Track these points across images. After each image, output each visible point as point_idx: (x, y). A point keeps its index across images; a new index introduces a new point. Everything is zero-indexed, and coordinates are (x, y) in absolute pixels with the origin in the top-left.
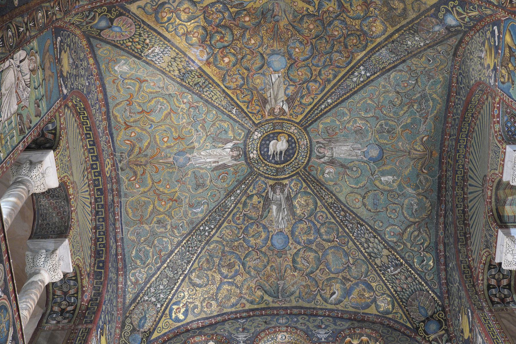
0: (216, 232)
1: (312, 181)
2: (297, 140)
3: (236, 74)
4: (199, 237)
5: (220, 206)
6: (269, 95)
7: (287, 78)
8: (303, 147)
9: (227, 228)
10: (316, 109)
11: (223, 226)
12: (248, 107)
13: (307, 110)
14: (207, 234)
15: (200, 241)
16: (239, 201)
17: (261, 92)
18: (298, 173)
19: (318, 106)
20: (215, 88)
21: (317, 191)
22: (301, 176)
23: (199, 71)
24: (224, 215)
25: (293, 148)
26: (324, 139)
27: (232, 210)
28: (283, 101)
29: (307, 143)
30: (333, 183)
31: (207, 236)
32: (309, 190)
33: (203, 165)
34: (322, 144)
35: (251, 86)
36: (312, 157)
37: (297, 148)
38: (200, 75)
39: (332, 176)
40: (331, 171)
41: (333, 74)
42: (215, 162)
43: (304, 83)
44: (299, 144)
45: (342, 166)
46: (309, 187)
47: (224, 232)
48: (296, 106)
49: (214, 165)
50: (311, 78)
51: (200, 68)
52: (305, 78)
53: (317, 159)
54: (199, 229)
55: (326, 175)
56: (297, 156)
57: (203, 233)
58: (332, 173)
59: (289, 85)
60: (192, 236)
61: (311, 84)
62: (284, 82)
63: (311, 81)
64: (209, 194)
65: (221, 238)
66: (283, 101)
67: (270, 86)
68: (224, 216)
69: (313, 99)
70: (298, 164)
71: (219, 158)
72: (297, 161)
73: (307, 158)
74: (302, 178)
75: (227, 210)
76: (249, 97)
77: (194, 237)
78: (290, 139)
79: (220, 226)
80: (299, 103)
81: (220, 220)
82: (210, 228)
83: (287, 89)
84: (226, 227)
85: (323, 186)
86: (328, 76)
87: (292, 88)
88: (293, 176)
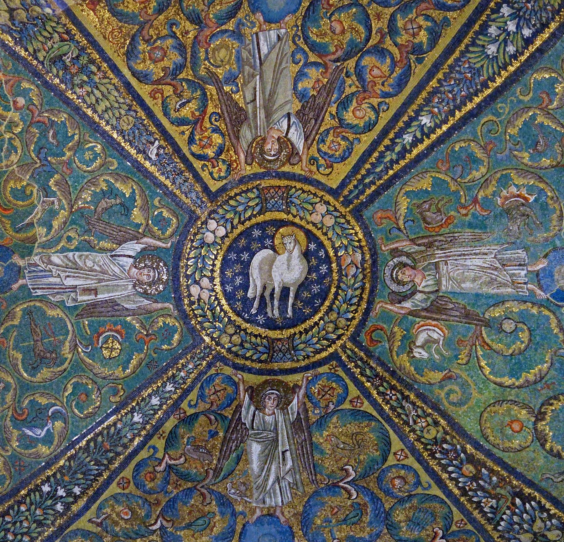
0: (87, 508)
1: (377, 375)
2: (336, 252)
3: (164, 38)
4: (38, 512)
5: (101, 433)
6: (249, 97)
7: (301, 42)
8: (353, 271)
9: (117, 501)
10: (387, 148)
11: (106, 494)
12: (191, 141)
13: (360, 149)
14: (59, 507)
15: (40, 524)
16: (156, 428)
17: (227, 88)
18: (334, 356)
19: (391, 135)
20: (105, 77)
21: (393, 408)
22: (343, 366)
23: (64, 20)
24: (111, 461)
25: (322, 278)
26: (412, 240)
27: (136, 452)
28: (289, 115)
29: (363, 259)
30: (437, 376)
31: (62, 515)
32: (367, 407)
33: (54, 295)
34: (408, 255)
35: (203, 73)
36: (377, 300)
37: (335, 276)
38: (68, 32)
39: (438, 351)
40: (435, 336)
41: (427, 29)
42: (87, 291)
43: (348, 56)
44: (339, 265)
45: (468, 316)
46: (368, 396)
47: (109, 510)
48: (328, 131)
49: (85, 298)
50: (368, 40)
51: (68, 12)
52: (351, 40)
53: (392, 303)
54: (38, 488)
55: (420, 353)
56: (333, 303)
57: (49, 502)
58: (436, 341)
59: (306, 65)
60: (20, 503)
61: (367, 61)
62: (293, 55)
63: (368, 52)
64: (70, 391)
65: (99, 525)
66: (289, 115)
67: (253, 67)
68: (112, 467)
69: (377, 112)
70: (337, 328)
71: (100, 281)
72: (333, 316)
73: (364, 305)
74: (348, 371)
75: (120, 449)
76: (193, 105)
77: (23, 508)
78: (312, 246)
79: (98, 494)
80: (335, 123)
81: (100, 475)
82: (69, 493)
83: (300, 75)
84: (114, 497)
85: (410, 387)
86: (414, 35)
87: (313, 73)
88: (320, 363)
